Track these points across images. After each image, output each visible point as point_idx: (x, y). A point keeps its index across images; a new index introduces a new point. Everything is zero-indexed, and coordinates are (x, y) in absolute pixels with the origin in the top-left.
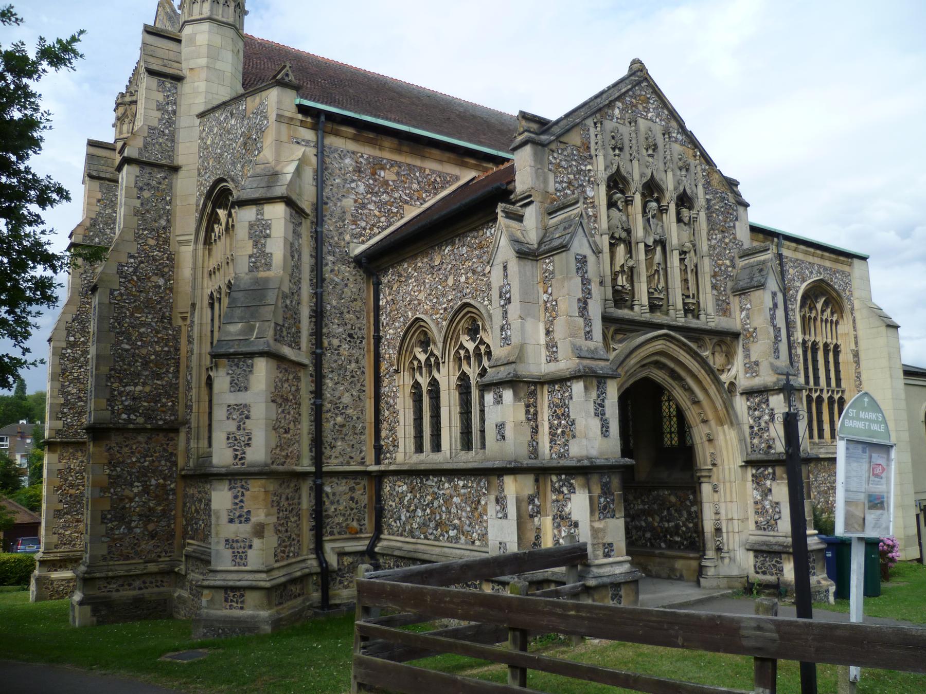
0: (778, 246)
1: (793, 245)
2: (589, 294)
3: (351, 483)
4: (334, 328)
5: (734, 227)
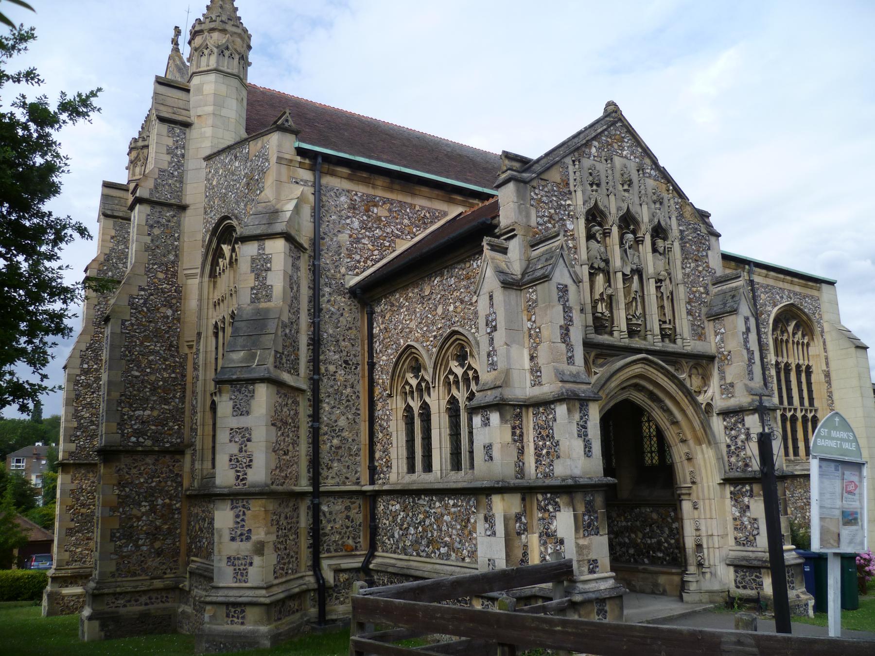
0: (750, 272)
1: (764, 271)
2: (571, 321)
3: (347, 502)
4: (331, 355)
5: (707, 256)
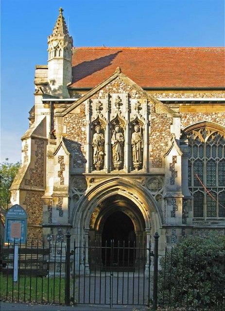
5: (169, 128)
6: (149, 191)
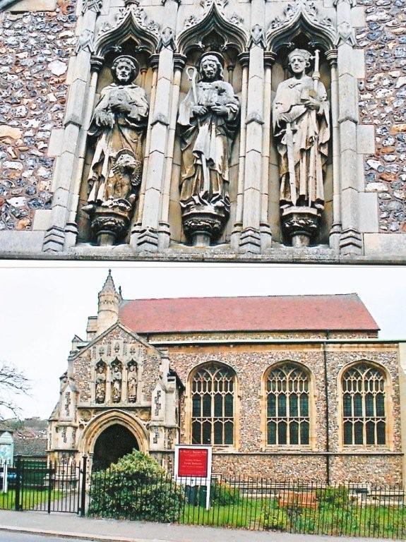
0: (324, 347)
1: (339, 345)
6: (141, 421)
